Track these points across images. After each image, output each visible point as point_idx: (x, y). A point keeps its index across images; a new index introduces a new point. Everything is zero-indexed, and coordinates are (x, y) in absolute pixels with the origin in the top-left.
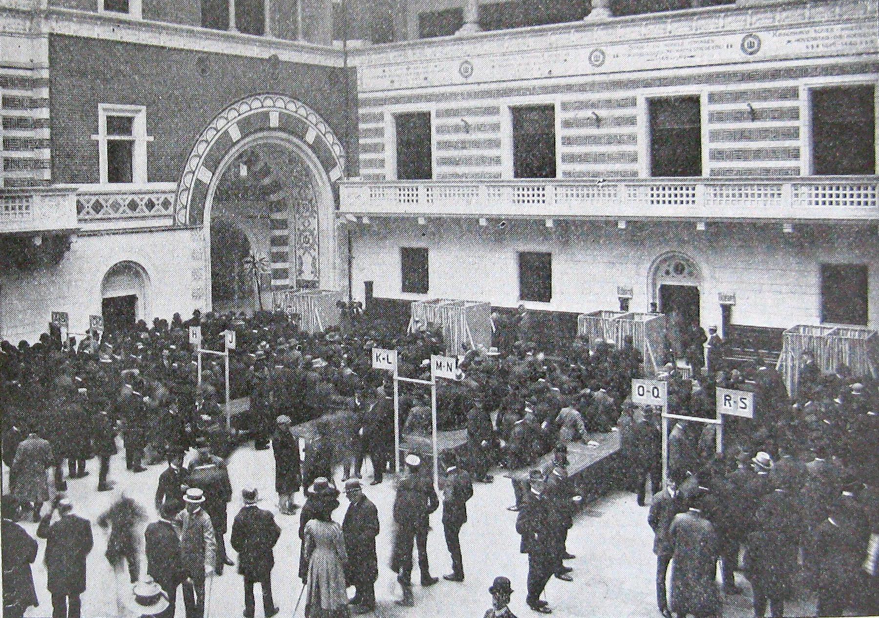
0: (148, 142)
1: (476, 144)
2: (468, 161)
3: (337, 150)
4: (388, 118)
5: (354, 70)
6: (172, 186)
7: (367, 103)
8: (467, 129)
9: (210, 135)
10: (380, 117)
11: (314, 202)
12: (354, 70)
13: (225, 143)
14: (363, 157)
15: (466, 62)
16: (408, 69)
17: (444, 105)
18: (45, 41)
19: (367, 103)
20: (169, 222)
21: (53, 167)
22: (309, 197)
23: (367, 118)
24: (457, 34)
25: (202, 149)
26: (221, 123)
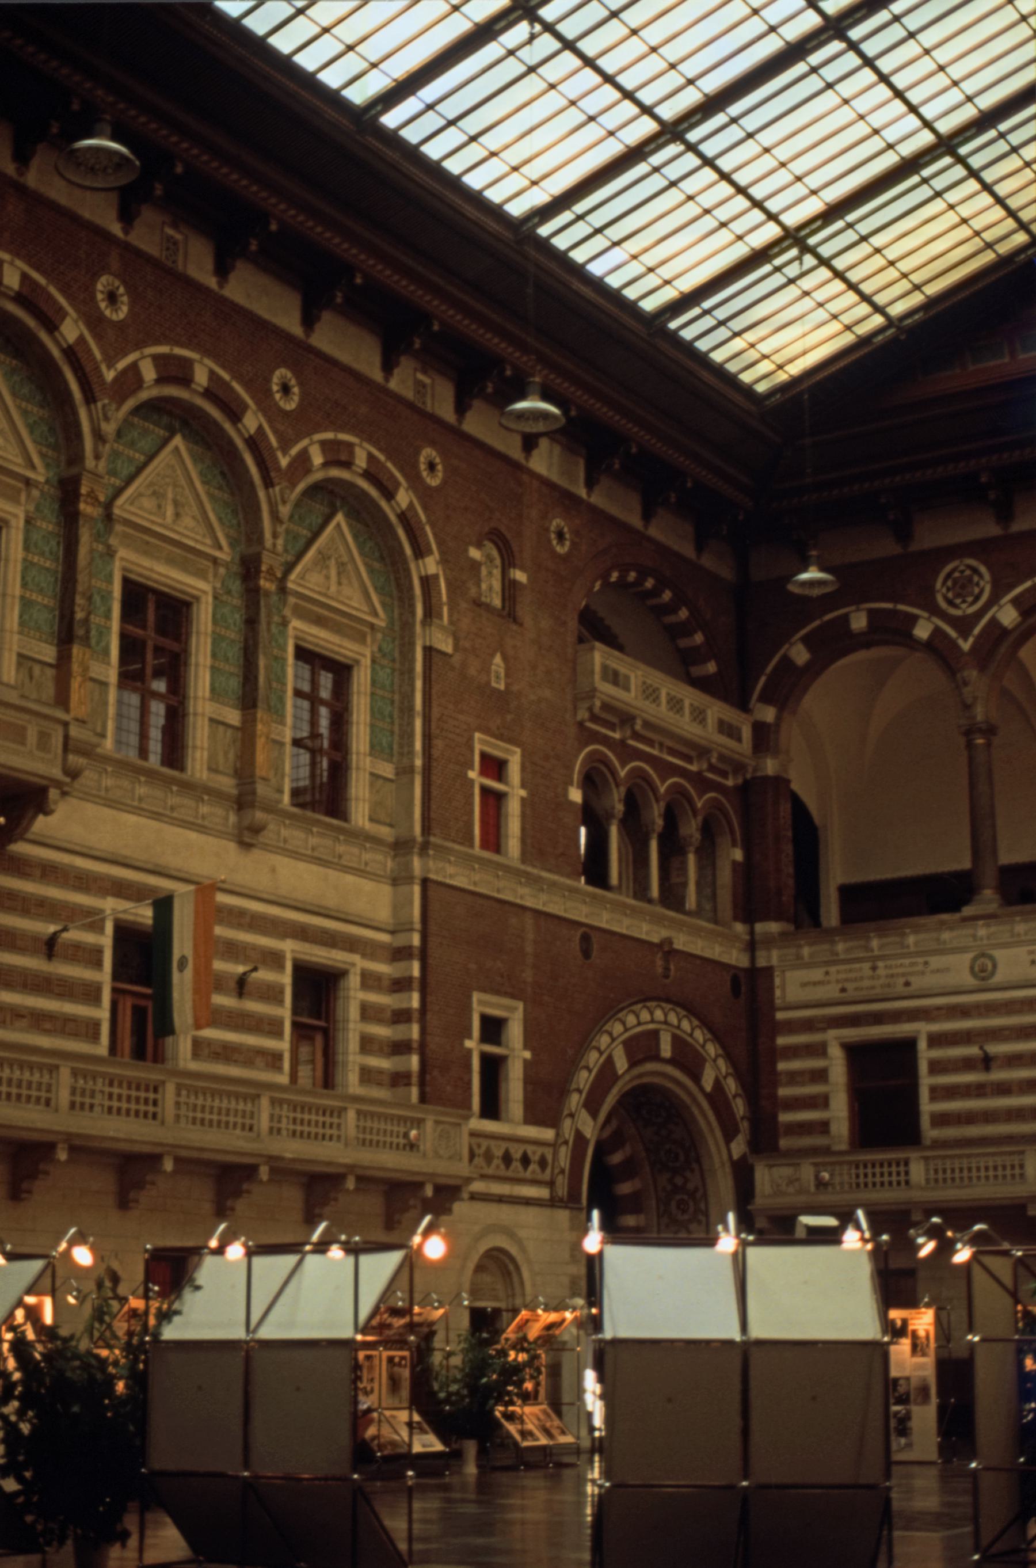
0: (525, 1061)
1: (1003, 1089)
2: (989, 1117)
3: (740, 1107)
4: (836, 1053)
5: (769, 971)
6: (548, 1134)
7: (791, 1027)
8: (987, 1062)
9: (593, 1058)
10: (819, 1050)
11: (699, 1195)
12: (769, 971)
13: (607, 1073)
14: (785, 1117)
15: (983, 955)
16: (874, 968)
17: (936, 1027)
18: (417, 889)
19: (791, 1027)
20: (543, 1193)
21: (422, 1084)
22: (690, 1186)
23: (794, 1052)
24: (967, 911)
25: (584, 1079)
26: (604, 1040)
